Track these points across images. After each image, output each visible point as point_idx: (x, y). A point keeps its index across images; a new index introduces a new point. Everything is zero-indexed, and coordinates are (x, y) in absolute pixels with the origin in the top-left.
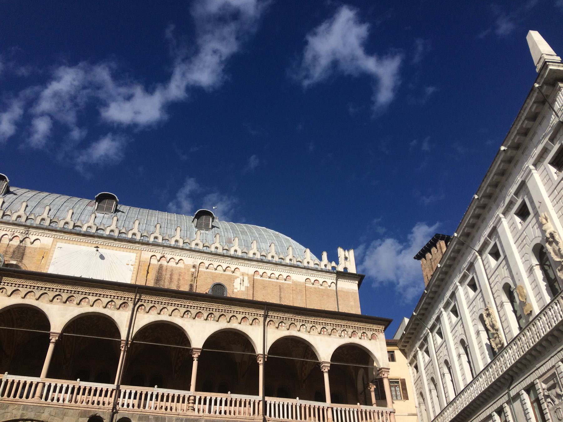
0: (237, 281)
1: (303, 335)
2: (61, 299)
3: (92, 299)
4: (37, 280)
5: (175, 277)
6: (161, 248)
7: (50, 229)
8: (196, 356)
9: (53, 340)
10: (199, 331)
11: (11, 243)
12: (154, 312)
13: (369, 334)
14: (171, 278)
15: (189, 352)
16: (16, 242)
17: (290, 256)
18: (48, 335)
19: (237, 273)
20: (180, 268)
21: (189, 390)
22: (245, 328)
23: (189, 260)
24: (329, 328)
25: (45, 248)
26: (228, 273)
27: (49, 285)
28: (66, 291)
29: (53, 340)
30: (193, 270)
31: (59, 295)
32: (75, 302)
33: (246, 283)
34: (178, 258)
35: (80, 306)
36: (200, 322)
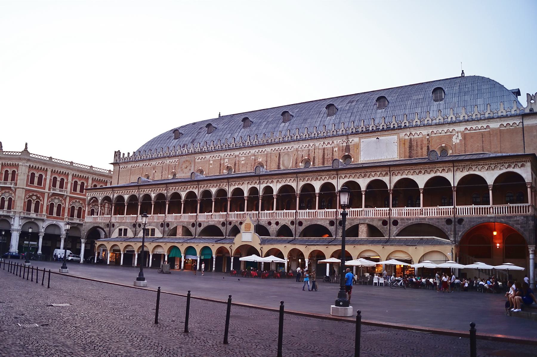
0: (454, 137)
1: (477, 173)
5: (419, 143)
6: (408, 129)
10: (422, 180)
12: (399, 175)
15: (418, 190)
16: (345, 144)
17: (489, 112)
18: (361, 191)
19: (454, 133)
21: (419, 206)
22: (443, 175)
23: (425, 132)
24: (493, 166)
30: (428, 137)
33: (460, 137)
34: (418, 132)
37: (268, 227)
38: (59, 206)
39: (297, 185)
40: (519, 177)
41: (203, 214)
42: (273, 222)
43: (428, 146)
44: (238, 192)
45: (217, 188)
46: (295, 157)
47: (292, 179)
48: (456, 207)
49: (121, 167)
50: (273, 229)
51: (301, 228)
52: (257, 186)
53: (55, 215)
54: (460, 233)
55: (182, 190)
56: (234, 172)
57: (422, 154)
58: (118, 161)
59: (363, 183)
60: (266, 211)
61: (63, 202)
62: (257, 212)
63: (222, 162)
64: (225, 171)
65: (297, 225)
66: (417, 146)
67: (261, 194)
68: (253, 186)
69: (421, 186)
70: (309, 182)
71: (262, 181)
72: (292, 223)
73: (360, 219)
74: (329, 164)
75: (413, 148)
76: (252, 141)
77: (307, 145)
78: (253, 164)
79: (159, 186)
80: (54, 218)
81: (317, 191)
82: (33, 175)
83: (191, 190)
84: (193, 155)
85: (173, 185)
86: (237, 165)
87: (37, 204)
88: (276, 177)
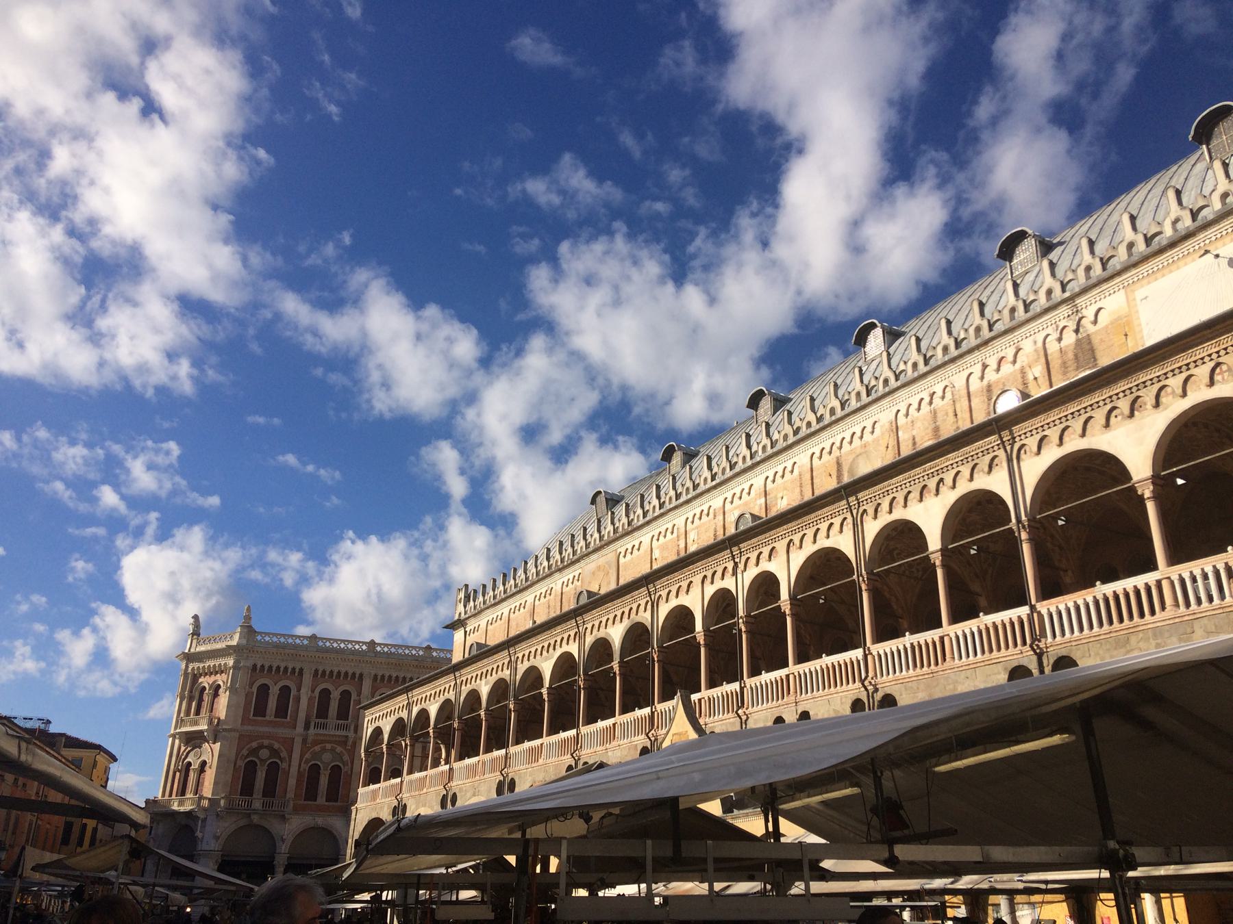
2: (1122, 414)
3: (1175, 382)
4: (1064, 403)
9: (1147, 494)
11: (1063, 343)
16: (1070, 338)
18: (1133, 489)
25: (1119, 318)
27: (1087, 401)
28: (1121, 395)
29: (1147, 494)
31: (1114, 408)
32: (1149, 406)
35: (1161, 407)
38: (336, 771)
45: (626, 623)
52: (729, 583)
53: (321, 800)
55: (545, 653)
59: (1134, 442)
60: (766, 677)
61: (346, 758)
68: (719, 584)
70: (899, 514)
73: (1157, 632)
80: (320, 809)
81: (934, 542)
82: (264, 690)
83: (565, 648)
84: (612, 547)
87: (273, 769)
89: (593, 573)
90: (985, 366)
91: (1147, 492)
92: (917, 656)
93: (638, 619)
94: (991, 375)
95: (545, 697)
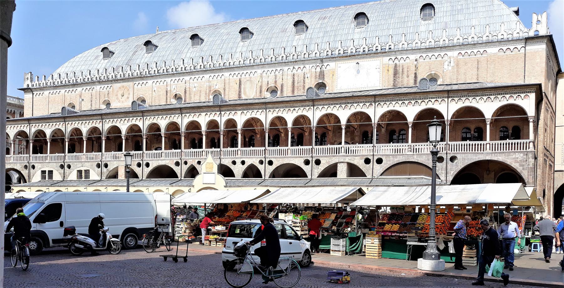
0: (446, 63)
5: (405, 70)
7: (333, 58)
8: (410, 125)
12: (385, 106)
13: (523, 95)
14: (403, 72)
16: (318, 70)
18: (341, 126)
19: (446, 58)
20: (407, 63)
23: (413, 57)
26: (439, 59)
30: (416, 63)
36: (410, 106)
37: (232, 167)
39: (266, 117)
40: (519, 110)
41: (150, 152)
42: (238, 161)
43: (415, 74)
44: (194, 125)
46: (260, 84)
47: (260, 111)
48: (449, 143)
49: (35, 93)
50: (238, 170)
51: (271, 169)
52: (217, 118)
54: (452, 172)
55: (122, 122)
56: (185, 101)
57: (407, 82)
58: (30, 86)
62: (219, 150)
63: (169, 89)
64: (174, 101)
65: (267, 165)
66: (403, 74)
67: (222, 129)
69: (410, 119)
71: (223, 113)
72: (261, 162)
74: (301, 94)
75: (398, 75)
76: (205, 63)
77: (274, 69)
78: (208, 92)
79: (91, 118)
81: (290, 125)
85: (109, 117)
86: (188, 92)
88: (240, 108)
89: (120, 88)
90: (294, 68)
91: (343, 127)
92: (280, 152)
93: (174, 120)
94: (294, 71)
95: (123, 138)
